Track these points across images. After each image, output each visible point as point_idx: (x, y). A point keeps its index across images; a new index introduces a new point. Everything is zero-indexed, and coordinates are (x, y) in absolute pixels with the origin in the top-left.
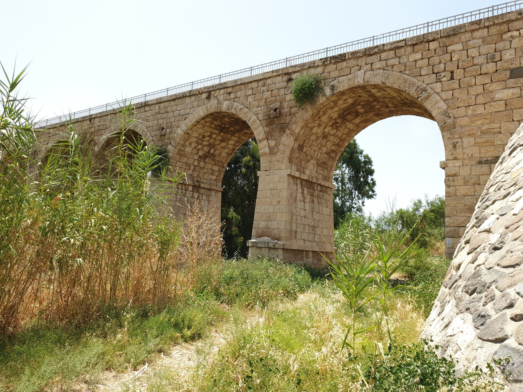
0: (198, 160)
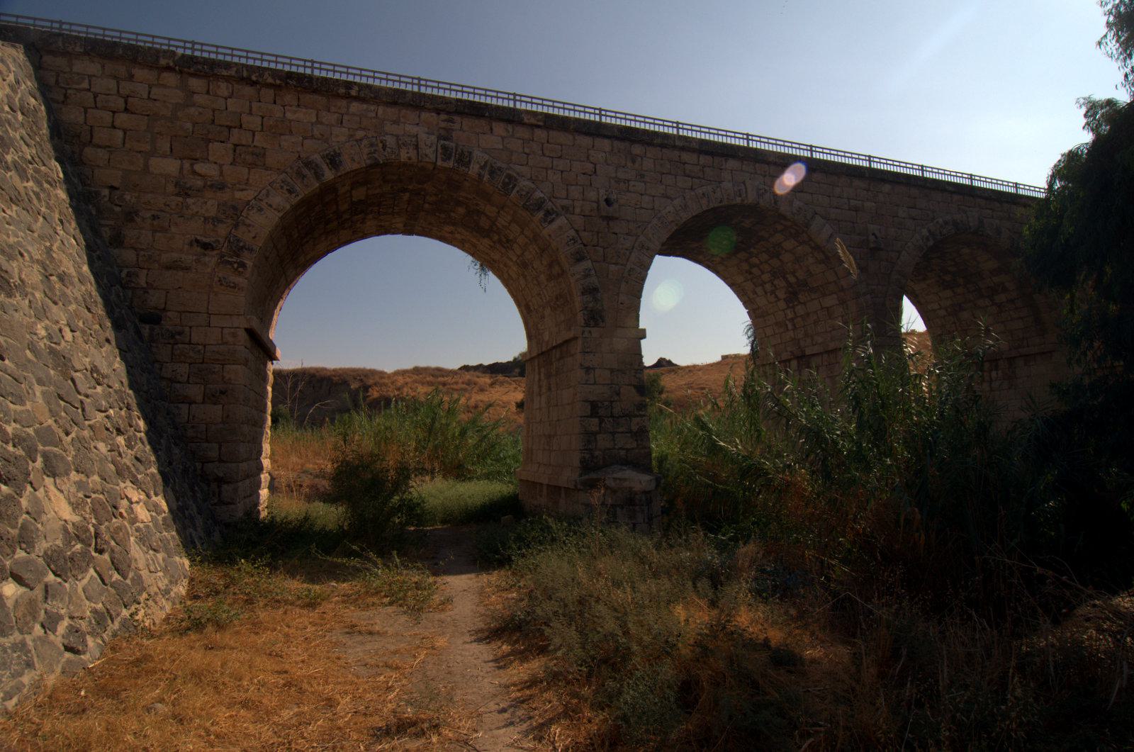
0: (788, 307)
